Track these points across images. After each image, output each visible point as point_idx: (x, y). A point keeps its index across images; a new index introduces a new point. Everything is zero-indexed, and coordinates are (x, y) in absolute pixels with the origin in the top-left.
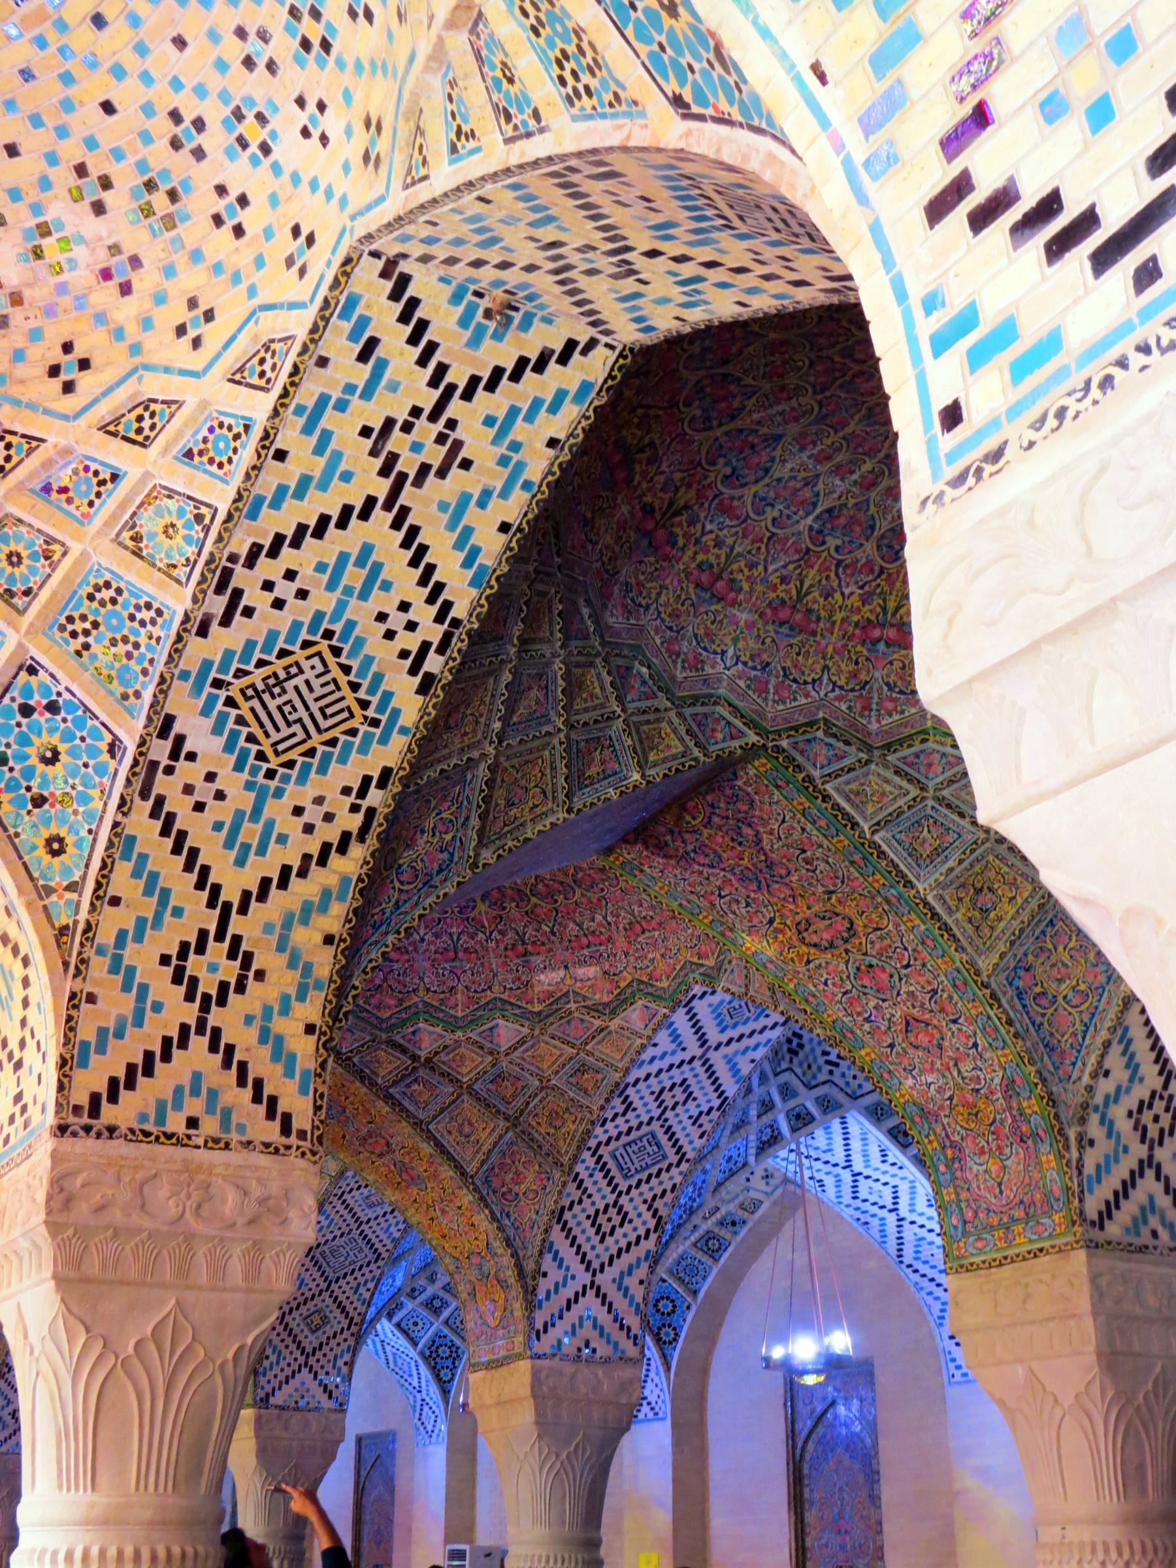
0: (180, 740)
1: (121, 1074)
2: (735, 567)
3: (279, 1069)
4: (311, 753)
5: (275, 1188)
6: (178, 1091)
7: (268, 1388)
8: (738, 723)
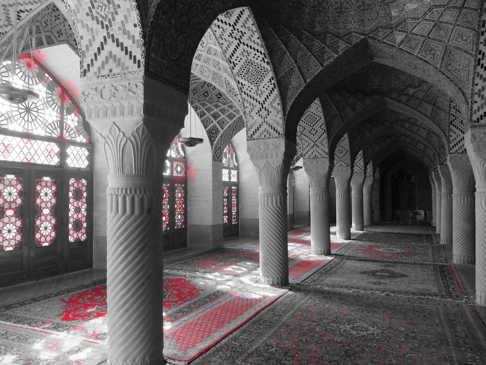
0: (242, 83)
1: (255, 131)
2: (344, 5)
3: (277, 125)
4: (260, 79)
5: (278, 143)
6: (263, 131)
7: (442, 161)
8: (358, 35)
